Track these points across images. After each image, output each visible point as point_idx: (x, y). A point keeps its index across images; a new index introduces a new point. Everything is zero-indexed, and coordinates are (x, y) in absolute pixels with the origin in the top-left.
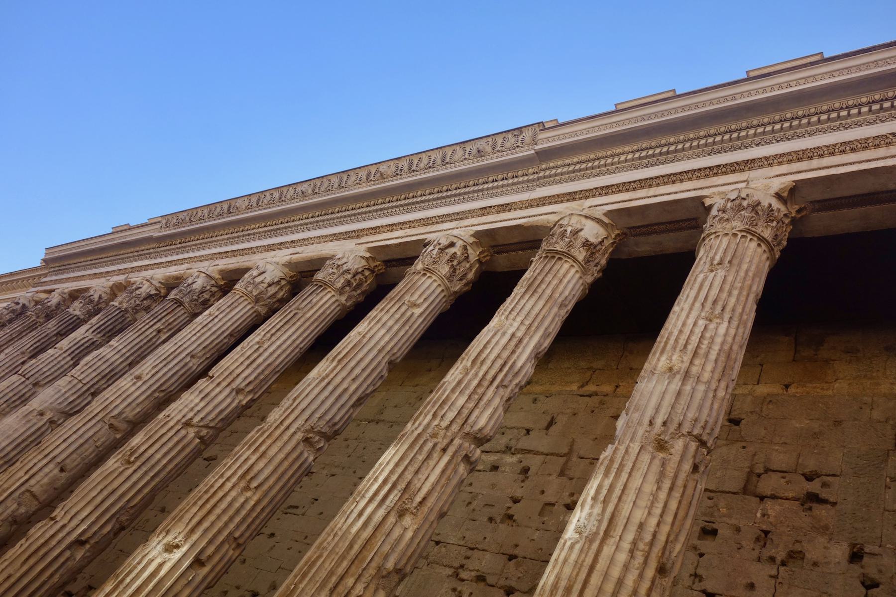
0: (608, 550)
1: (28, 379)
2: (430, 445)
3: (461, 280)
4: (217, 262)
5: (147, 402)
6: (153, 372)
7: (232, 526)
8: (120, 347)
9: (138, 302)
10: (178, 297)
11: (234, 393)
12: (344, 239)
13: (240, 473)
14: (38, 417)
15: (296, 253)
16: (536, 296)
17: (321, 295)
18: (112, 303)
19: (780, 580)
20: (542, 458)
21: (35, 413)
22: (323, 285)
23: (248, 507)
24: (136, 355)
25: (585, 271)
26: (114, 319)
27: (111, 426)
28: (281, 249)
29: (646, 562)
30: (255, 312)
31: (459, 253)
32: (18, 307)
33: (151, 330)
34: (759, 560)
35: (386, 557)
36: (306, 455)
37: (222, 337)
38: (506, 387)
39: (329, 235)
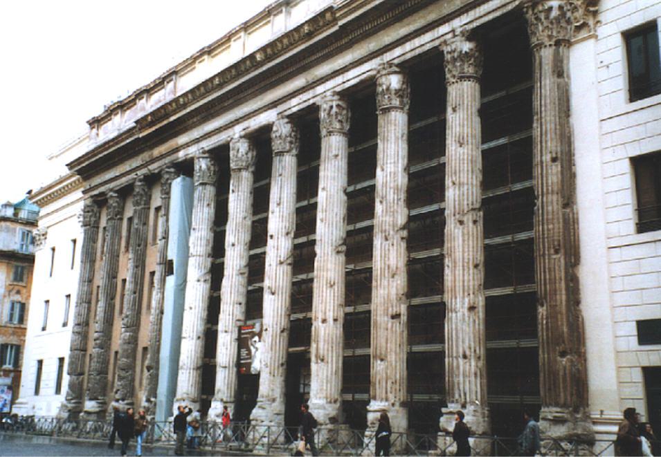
0: (457, 272)
2: (387, 246)
7: (336, 302)
10: (201, 181)
13: (325, 283)
16: (389, 142)
22: (281, 153)
25: (402, 109)
27: (241, 274)
29: (469, 268)
31: (338, 110)
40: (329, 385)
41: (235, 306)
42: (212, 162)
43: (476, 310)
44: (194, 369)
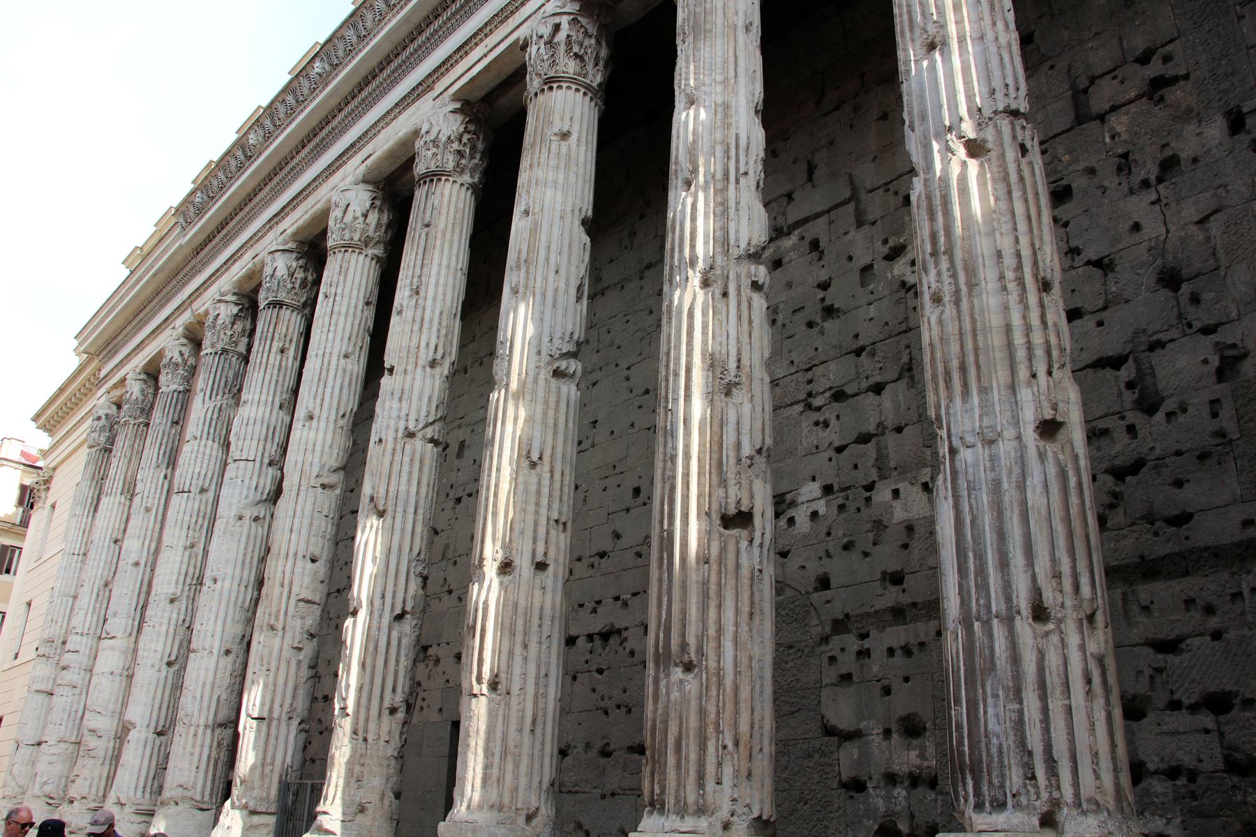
1: (189, 492)
3: (596, 65)
4: (281, 227)
5: (337, 437)
6: (318, 401)
7: (544, 511)
8: (257, 397)
9: (229, 333)
11: (428, 369)
12: (413, 101)
14: (239, 523)
15: (369, 157)
17: (438, 191)
18: (203, 353)
19: (1164, 201)
20: (824, 219)
21: (232, 521)
22: (434, 176)
23: (546, 482)
24: (278, 393)
26: (220, 369)
27: (324, 486)
28: (345, 163)
30: (372, 259)
32: (103, 422)
33: (272, 356)
34: (1132, 192)
35: (738, 446)
36: (564, 389)
37: (359, 313)
38: (746, 173)
39: (391, 109)
40: (510, 767)
41: (300, 563)
42: (301, 262)
43: (1061, 435)
44: (206, 726)
